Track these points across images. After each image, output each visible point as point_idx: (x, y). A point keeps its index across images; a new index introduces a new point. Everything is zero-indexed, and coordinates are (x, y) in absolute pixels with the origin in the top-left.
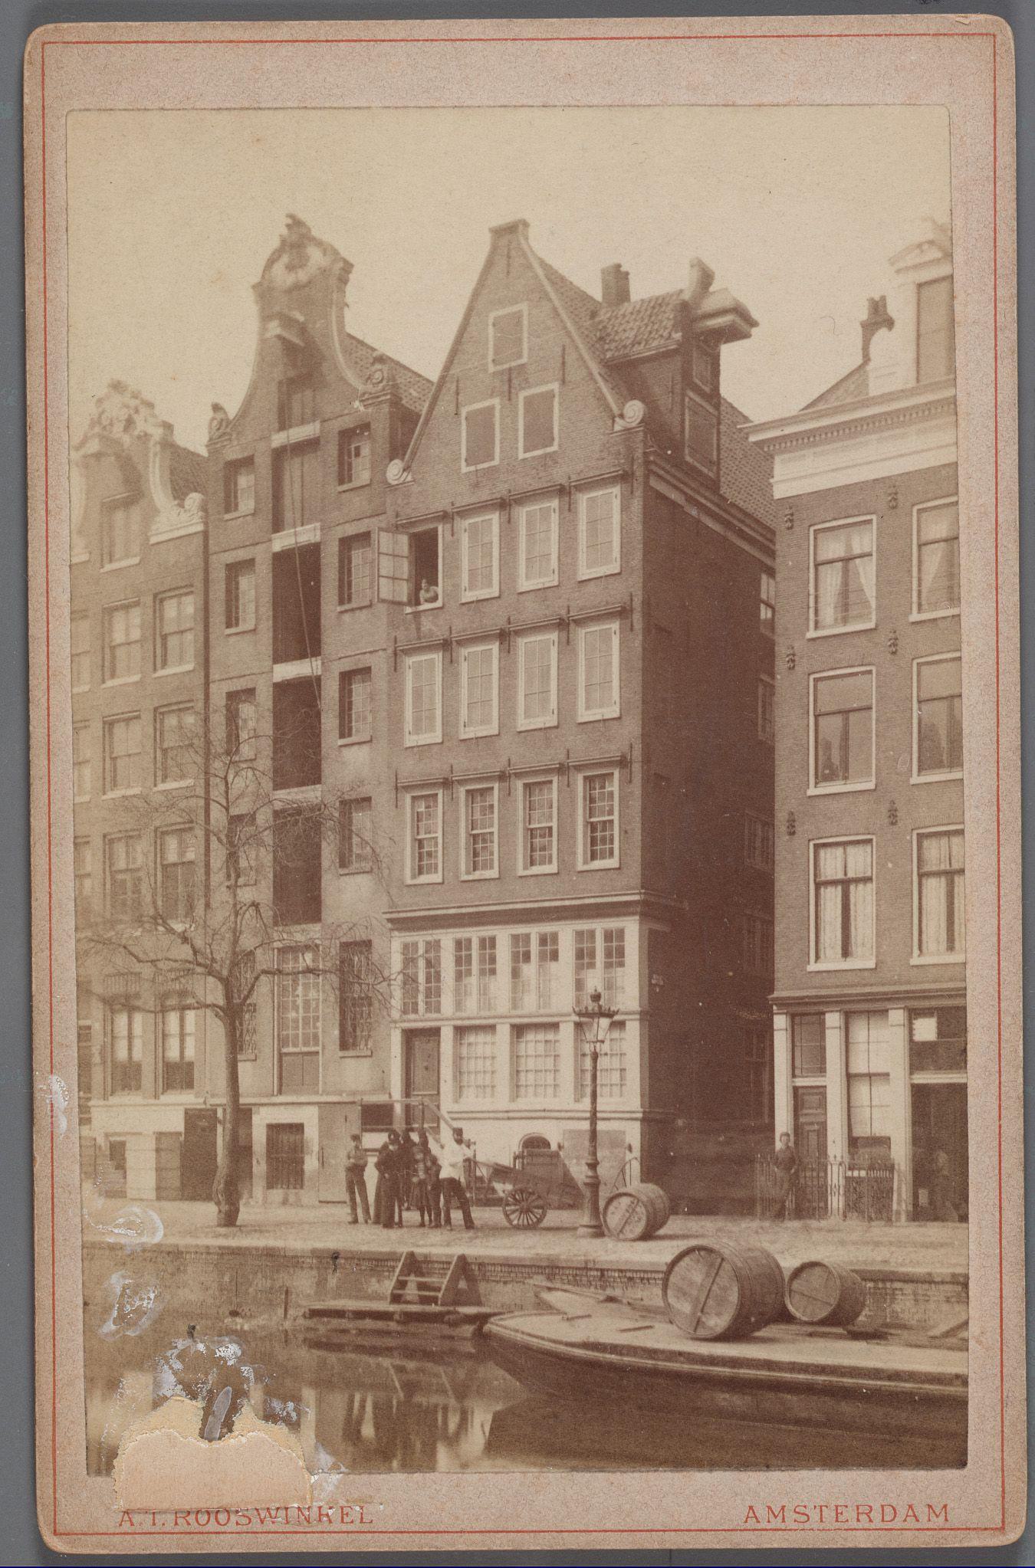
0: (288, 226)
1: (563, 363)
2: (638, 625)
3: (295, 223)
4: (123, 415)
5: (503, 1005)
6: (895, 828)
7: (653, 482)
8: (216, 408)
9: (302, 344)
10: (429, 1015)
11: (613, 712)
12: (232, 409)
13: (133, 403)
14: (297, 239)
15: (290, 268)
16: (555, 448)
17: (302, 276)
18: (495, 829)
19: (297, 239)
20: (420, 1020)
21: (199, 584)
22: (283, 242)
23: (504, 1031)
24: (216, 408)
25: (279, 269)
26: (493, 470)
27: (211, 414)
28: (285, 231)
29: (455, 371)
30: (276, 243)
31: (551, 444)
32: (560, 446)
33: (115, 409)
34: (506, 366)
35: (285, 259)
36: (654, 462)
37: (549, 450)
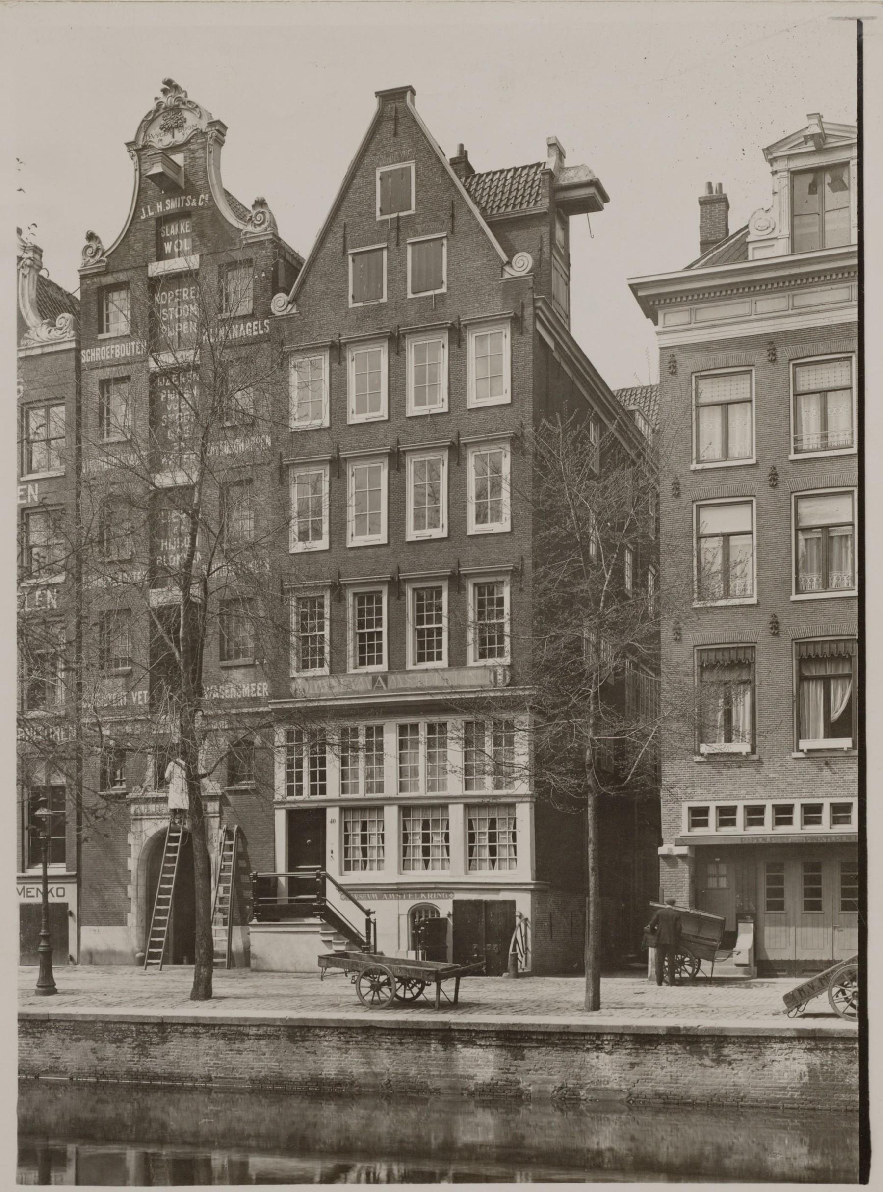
0: (165, 91)
1: (453, 216)
3: (170, 86)
5: (391, 789)
6: (776, 639)
7: (539, 327)
8: (91, 237)
9: (184, 187)
10: (313, 797)
11: (504, 526)
12: (109, 239)
14: (172, 105)
16: (444, 290)
17: (180, 137)
18: (384, 629)
19: (172, 105)
21: (71, 393)
22: (159, 105)
24: (91, 237)
27: (86, 243)
28: (160, 95)
30: (152, 106)
31: (440, 285)
32: (448, 288)
34: (394, 215)
35: (160, 121)
36: (540, 308)
37: (437, 292)
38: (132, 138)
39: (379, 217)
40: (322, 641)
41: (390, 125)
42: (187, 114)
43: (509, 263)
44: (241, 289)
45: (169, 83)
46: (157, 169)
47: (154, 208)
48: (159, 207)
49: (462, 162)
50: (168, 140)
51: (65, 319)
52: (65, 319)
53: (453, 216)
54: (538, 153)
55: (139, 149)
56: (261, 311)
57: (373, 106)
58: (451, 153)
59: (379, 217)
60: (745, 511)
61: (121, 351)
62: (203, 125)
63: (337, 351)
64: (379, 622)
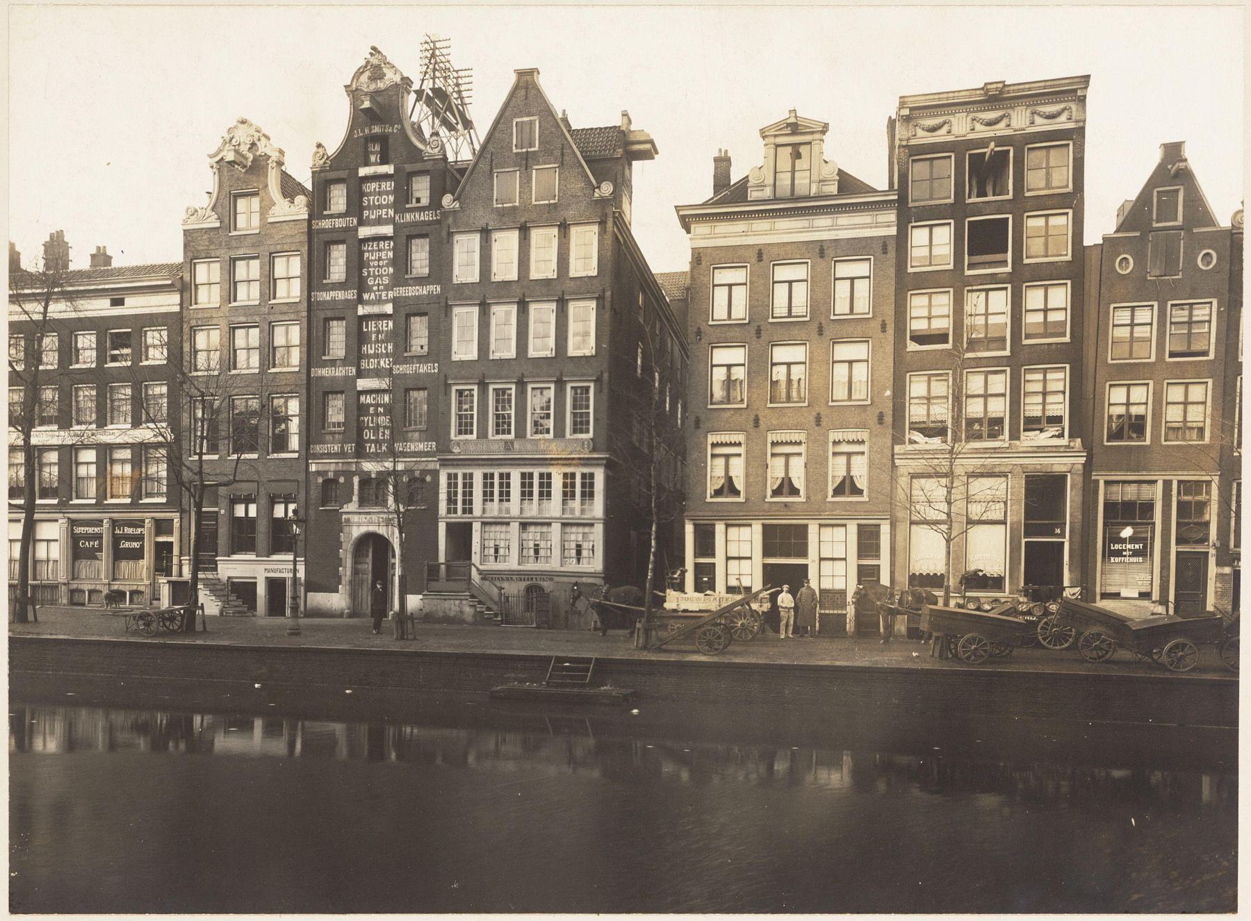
0: (372, 54)
2: (608, 305)
4: (249, 141)
8: (319, 146)
12: (333, 147)
13: (256, 135)
15: (373, 79)
17: (381, 85)
20: (459, 517)
22: (368, 62)
23: (515, 526)
24: (319, 146)
25: (364, 78)
26: (514, 208)
27: (315, 149)
29: (490, 147)
30: (363, 63)
33: (243, 136)
35: (367, 74)
38: (348, 83)
39: (515, 150)
40: (509, 417)
41: (523, 92)
42: (385, 70)
43: (599, 187)
44: (422, 189)
45: (374, 48)
46: (367, 104)
47: (363, 131)
48: (367, 131)
49: (565, 120)
50: (373, 87)
51: (301, 200)
52: (301, 200)
53: (563, 154)
54: (617, 121)
55: (353, 93)
56: (435, 203)
57: (512, 80)
58: (560, 116)
59: (515, 150)
60: (864, 347)
61: (340, 223)
62: (397, 79)
63: (486, 233)
64: (587, 407)
